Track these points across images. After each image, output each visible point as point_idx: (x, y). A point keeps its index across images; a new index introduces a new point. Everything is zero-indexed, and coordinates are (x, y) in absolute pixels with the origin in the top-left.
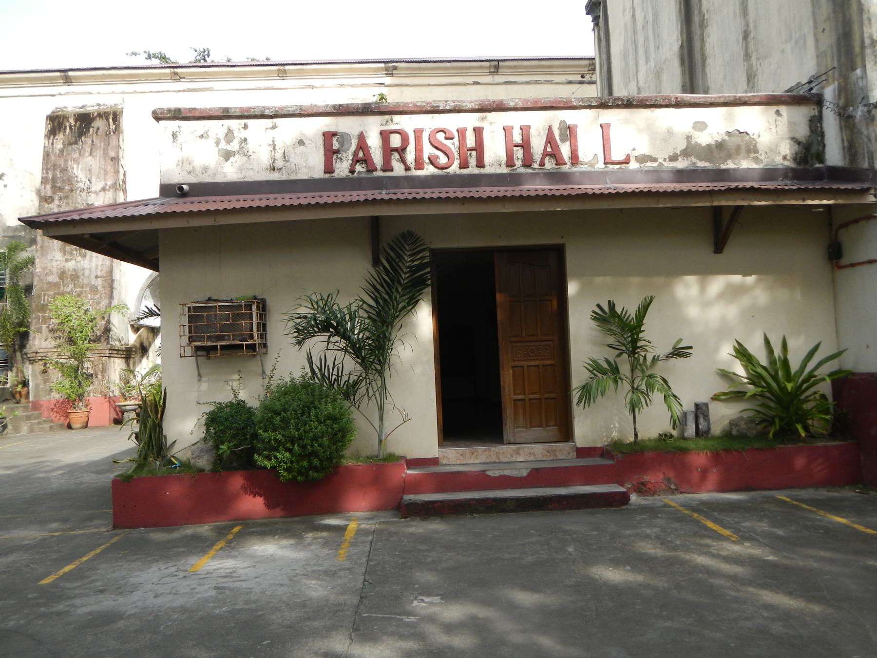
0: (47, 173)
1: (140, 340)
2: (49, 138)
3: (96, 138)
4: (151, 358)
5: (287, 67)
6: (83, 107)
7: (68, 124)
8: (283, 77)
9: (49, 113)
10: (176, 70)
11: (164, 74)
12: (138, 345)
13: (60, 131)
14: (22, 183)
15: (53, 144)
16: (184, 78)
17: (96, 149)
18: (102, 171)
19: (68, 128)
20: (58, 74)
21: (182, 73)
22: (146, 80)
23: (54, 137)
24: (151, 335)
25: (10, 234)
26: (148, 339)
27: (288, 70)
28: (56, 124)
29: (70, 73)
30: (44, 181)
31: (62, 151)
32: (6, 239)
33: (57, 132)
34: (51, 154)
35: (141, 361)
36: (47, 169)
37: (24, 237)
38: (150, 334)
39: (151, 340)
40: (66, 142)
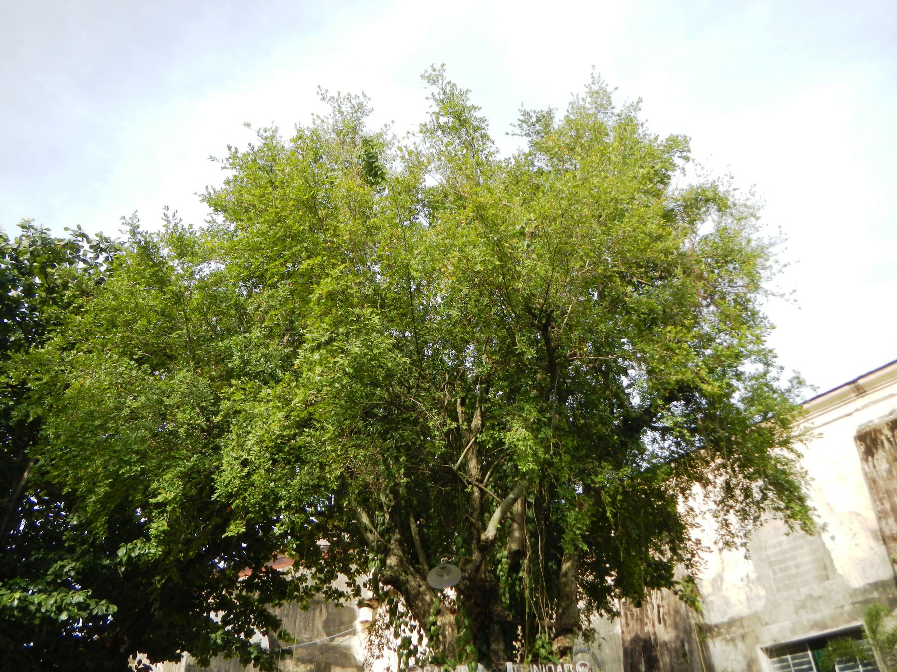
0: (882, 504)
2: (867, 461)
6: (891, 413)
7: (883, 438)
9: (854, 433)
13: (876, 448)
14: (851, 529)
15: (874, 467)
19: (885, 442)
20: (847, 388)
23: (873, 457)
25: (860, 598)
28: (868, 441)
29: (861, 382)
30: (881, 516)
31: (890, 472)
32: (857, 606)
33: (874, 451)
34: (877, 479)
36: (880, 500)
37: (879, 599)
40: (891, 459)
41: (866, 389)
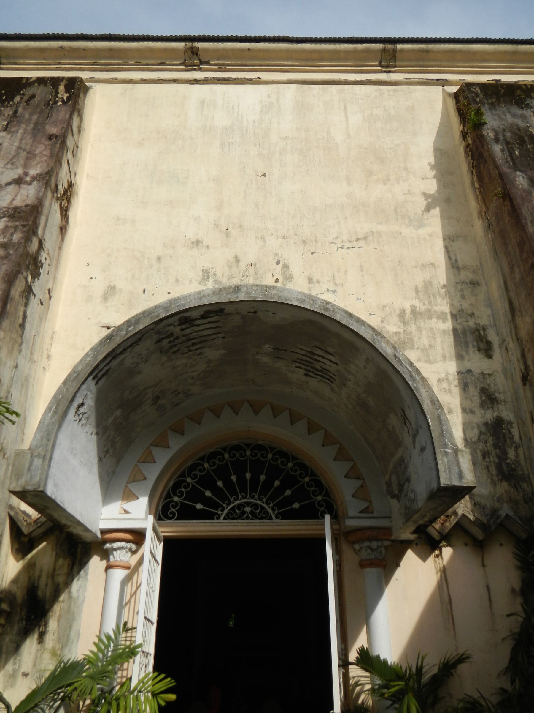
1: (30, 578)
3: (24, 109)
4: (50, 640)
5: (399, 46)
8: (387, 67)
10: (196, 44)
11: (173, 50)
12: (20, 595)
16: (207, 63)
17: (20, 123)
18: (23, 154)
21: (206, 50)
22: (138, 63)
24: (63, 563)
26: (53, 575)
27: (402, 50)
35: (17, 647)
38: (61, 561)
39: (61, 579)
41: (3, 61)
